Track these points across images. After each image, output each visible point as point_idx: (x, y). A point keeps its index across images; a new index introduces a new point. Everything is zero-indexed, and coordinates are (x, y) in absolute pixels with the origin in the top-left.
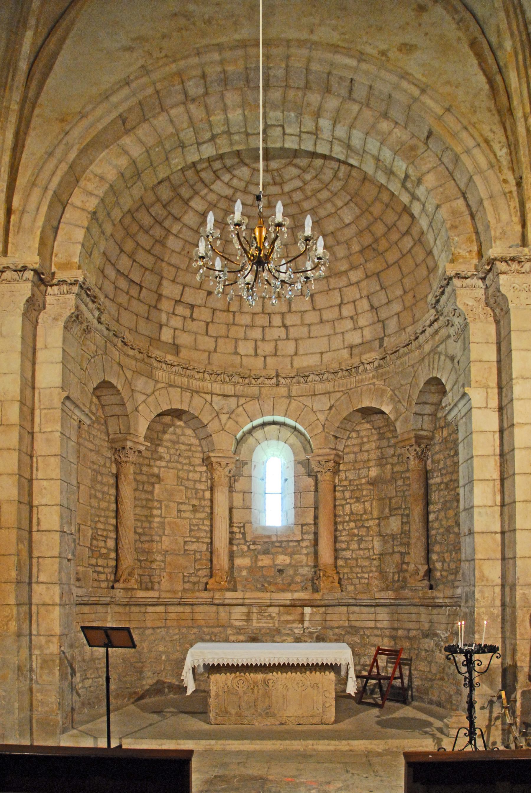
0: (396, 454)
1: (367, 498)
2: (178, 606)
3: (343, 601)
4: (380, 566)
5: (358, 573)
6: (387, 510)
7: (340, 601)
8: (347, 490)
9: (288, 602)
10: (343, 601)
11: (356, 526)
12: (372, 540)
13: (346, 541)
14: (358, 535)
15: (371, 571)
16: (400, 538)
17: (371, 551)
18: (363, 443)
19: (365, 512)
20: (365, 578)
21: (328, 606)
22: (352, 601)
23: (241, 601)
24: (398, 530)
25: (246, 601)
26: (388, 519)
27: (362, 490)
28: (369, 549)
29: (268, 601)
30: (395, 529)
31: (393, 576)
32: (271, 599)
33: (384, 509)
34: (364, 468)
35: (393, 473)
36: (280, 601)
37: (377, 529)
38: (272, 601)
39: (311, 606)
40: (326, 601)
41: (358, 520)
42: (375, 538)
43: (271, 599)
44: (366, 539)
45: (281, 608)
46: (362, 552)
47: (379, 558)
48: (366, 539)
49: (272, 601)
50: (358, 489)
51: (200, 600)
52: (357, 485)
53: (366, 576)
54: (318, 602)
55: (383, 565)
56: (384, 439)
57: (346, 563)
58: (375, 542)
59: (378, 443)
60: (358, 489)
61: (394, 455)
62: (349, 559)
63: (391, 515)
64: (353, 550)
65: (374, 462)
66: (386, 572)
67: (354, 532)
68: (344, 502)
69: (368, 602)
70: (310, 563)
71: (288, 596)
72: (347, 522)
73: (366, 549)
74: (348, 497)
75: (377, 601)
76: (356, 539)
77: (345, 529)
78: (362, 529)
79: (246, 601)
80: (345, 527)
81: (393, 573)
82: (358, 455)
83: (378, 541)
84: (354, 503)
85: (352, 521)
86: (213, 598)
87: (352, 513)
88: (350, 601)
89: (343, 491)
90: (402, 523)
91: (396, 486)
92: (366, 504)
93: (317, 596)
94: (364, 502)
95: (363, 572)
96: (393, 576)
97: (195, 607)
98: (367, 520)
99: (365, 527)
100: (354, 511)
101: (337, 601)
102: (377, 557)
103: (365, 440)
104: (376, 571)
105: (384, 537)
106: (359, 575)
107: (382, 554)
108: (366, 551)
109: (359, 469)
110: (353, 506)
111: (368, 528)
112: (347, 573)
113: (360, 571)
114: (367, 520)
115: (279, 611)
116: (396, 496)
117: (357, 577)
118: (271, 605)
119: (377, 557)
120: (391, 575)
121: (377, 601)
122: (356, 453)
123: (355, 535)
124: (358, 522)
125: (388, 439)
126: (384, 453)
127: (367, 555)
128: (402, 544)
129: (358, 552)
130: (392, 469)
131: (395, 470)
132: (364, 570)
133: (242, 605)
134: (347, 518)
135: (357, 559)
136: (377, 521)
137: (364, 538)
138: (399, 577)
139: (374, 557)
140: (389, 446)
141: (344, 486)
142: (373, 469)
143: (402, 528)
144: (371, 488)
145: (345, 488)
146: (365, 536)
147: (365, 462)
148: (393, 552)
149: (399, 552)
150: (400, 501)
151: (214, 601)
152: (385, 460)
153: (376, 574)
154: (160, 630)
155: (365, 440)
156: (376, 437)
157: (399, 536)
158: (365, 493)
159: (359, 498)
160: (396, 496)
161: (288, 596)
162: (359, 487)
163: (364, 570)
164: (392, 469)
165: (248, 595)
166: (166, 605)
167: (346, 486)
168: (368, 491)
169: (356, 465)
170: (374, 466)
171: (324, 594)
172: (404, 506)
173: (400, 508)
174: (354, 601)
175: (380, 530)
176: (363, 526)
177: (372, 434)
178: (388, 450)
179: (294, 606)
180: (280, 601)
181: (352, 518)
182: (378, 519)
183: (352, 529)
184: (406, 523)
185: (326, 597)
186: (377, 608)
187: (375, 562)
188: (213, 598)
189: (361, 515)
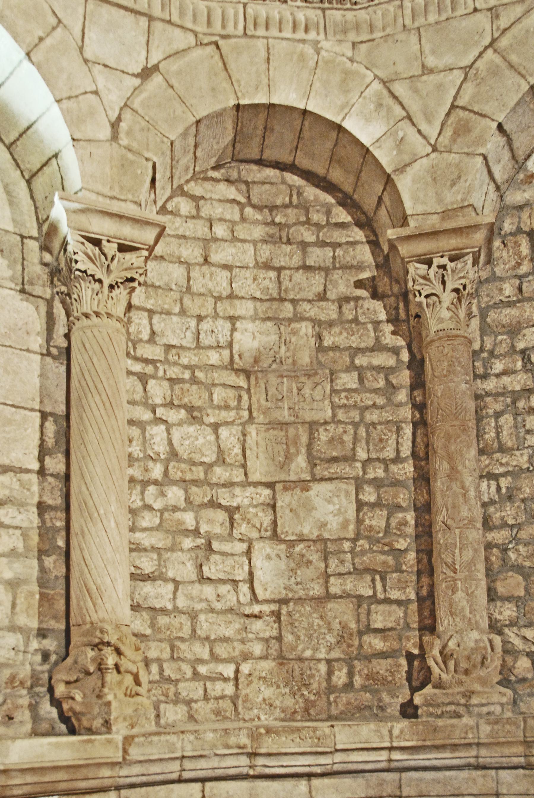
0: (332, 295)
1: (231, 415)
4: (279, 639)
5: (200, 661)
6: (301, 461)
8: (154, 377)
11: (188, 500)
12: (248, 553)
13: (153, 548)
14: (196, 532)
15: (246, 657)
16: (352, 551)
17: (244, 588)
18: (216, 240)
19: (221, 460)
20: (226, 680)
24: (345, 525)
26: (306, 489)
27: (210, 387)
28: (235, 582)
30: (334, 523)
31: (330, 673)
33: (288, 458)
34: (216, 316)
35: (321, 349)
37: (266, 519)
41: (195, 482)
42: (257, 546)
44: (226, 547)
46: (208, 591)
47: (277, 615)
48: (226, 547)
50: (194, 380)
52: (191, 368)
53: (229, 670)
55: (289, 638)
56: (289, 242)
57: (152, 625)
58: (258, 561)
59: (265, 251)
60: (194, 380)
61: (322, 297)
62: (163, 611)
63: (314, 479)
64: (176, 583)
65: (250, 304)
66: (301, 659)
67: (180, 523)
68: (147, 416)
70: (22, 620)
72: (156, 483)
73: (223, 581)
74: (158, 401)
76: (188, 543)
77: (149, 507)
78: (210, 513)
80: (149, 500)
81: (329, 662)
82: (195, 273)
83: (268, 557)
84: (180, 424)
85: (175, 483)
87: (173, 454)
89: (143, 379)
90: (360, 505)
91: (334, 391)
92: (224, 432)
94: (215, 427)
95: (215, 658)
96: (330, 673)
98: (229, 485)
99: (220, 506)
100: (180, 450)
102: (266, 608)
103: (220, 231)
104: (265, 657)
105: (291, 544)
106: (202, 670)
107: (284, 601)
108: (224, 589)
109: (200, 318)
110: (176, 434)
111: (231, 511)
112: (159, 660)
113: (205, 655)
114: (229, 485)
116: (334, 420)
117: (196, 675)
119: (266, 608)
120: (323, 668)
122: (188, 265)
123: (186, 533)
124: (194, 489)
125: (304, 245)
126: (286, 283)
127: (231, 600)
128: (357, 572)
129: (196, 589)
130: (319, 337)
131: (328, 342)
132: (222, 650)
134: (157, 472)
135: (193, 616)
136: (267, 492)
137: (215, 545)
138: (351, 674)
139: (256, 609)
140: (306, 268)
141: (146, 361)
142: (250, 326)
143: (359, 522)
144: (242, 382)
145: (149, 369)
146: (220, 538)
147: (218, 299)
148: (329, 597)
149: (346, 596)
150: (348, 438)
152: (288, 306)
153: (267, 665)
155: (220, 231)
156: (258, 232)
157: (347, 546)
158: (219, 395)
159: (200, 409)
160: (334, 420)
162: (200, 375)
163: (222, 650)
164: (319, 337)
167: (153, 362)
168: (232, 393)
169: (187, 301)
170: (254, 318)
172: (362, 455)
173: (350, 459)
175: (275, 523)
176: (213, 504)
177: (243, 219)
178: (299, 276)
181: (175, 473)
182: (271, 485)
183: (175, 509)
184: (373, 506)
187: (258, 625)
189: (209, 467)
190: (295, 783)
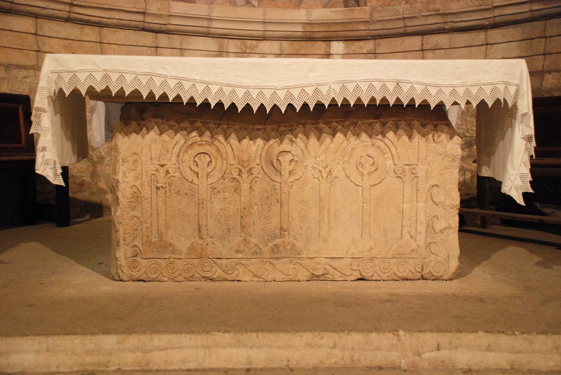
2: (68, 25)
3: (416, 22)
7: (408, 23)
9: (299, 28)
10: (416, 22)
21: (381, 37)
22: (434, 21)
23: (205, 24)
25: (215, 24)
29: (260, 27)
32: (265, 23)
36: (282, 28)
38: (269, 27)
39: (347, 39)
40: (379, 26)
43: (265, 23)
45: (285, 44)
49: (269, 27)
51: (116, 15)
54: (362, 27)
69: (474, 19)
71: (301, 15)
75: (497, 12)
79: (215, 24)
86: (144, 13)
88: (431, 20)
93: (359, 13)
97: (105, 31)
101: (400, 24)
115: (281, 48)
118: (264, 38)
121: (497, 12)
133: (207, 35)
151: (148, 19)
154: (23, 73)
161: (301, 15)
165: (218, 11)
166: (36, 16)
171: (373, 9)
174: (439, 19)
179: (310, 39)
180: (282, 28)
185: (377, 16)
186: (491, 32)
188: (144, 13)
190: (477, 34)
